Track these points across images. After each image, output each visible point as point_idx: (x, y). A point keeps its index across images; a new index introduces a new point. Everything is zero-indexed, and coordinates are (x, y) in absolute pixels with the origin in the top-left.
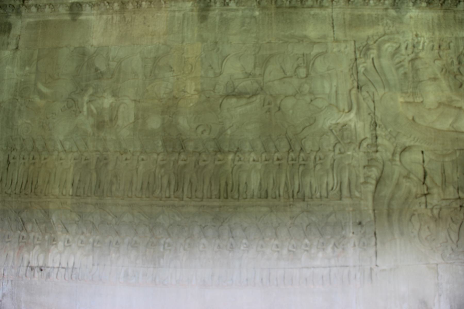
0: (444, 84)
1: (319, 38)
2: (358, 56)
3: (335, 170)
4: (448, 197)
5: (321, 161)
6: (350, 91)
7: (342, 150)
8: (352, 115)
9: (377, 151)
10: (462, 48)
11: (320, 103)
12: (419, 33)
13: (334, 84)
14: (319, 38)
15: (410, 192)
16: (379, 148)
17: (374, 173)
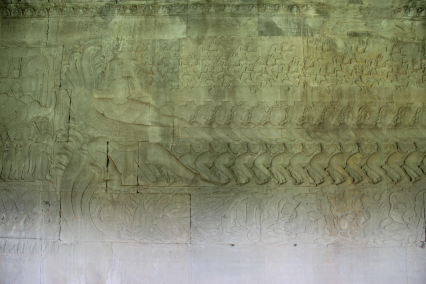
0: (136, 82)
1: (34, 44)
2: (64, 58)
3: (31, 156)
4: (127, 184)
5: (21, 148)
6: (53, 88)
7: (39, 140)
8: (51, 110)
9: (68, 141)
10: (158, 49)
11: (26, 100)
12: (120, 37)
13: (40, 83)
14: (34, 44)
15: (94, 178)
16: (70, 138)
17: (65, 160)
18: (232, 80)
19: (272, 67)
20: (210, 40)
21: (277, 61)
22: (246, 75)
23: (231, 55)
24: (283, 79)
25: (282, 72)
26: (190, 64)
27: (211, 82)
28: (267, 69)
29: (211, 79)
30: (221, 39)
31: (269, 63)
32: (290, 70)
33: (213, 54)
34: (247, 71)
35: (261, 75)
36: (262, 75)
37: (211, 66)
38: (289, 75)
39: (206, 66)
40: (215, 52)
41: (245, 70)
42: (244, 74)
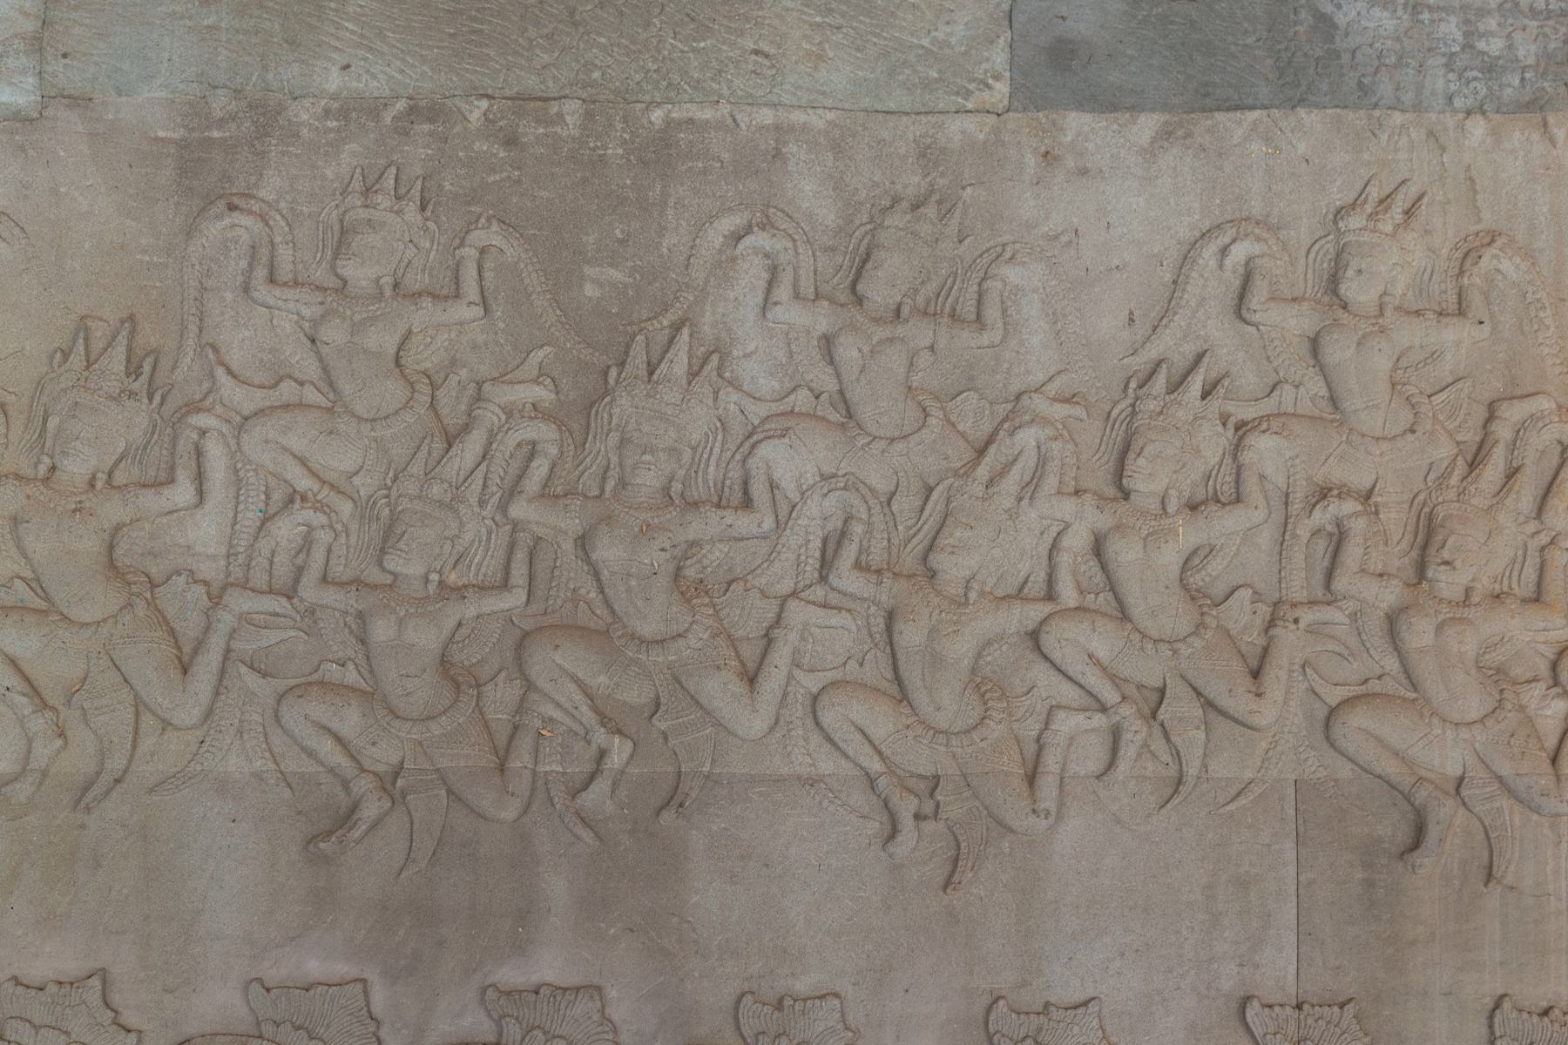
18: (636, 694)
19: (1187, 534)
20: (351, 154)
21: (1267, 453)
22: (829, 635)
23: (638, 357)
24: (1334, 696)
25: (1329, 595)
26: (76, 467)
27: (350, 721)
28: (1126, 553)
29: (352, 676)
30: (511, 141)
31: (1148, 478)
32: (1448, 583)
33: (383, 340)
34: (847, 578)
35: (1034, 636)
36: (1049, 641)
37: (365, 511)
38: (1420, 633)
39: (293, 498)
40: (424, 315)
41: (826, 564)
42: (798, 613)
